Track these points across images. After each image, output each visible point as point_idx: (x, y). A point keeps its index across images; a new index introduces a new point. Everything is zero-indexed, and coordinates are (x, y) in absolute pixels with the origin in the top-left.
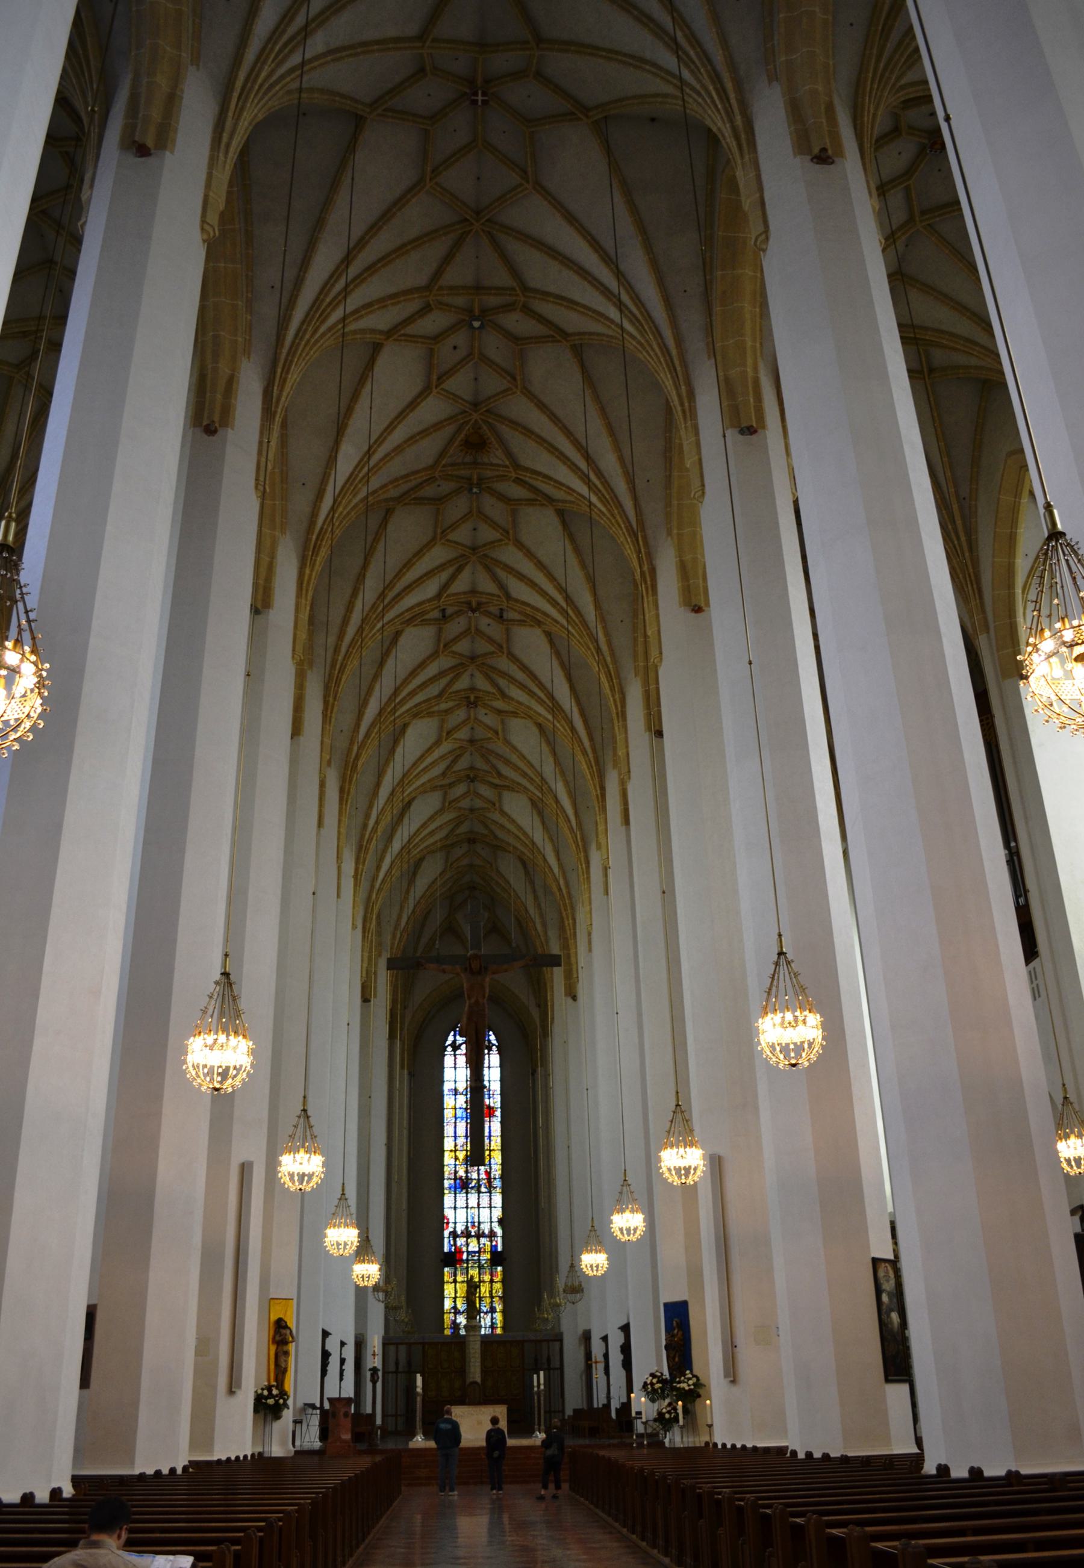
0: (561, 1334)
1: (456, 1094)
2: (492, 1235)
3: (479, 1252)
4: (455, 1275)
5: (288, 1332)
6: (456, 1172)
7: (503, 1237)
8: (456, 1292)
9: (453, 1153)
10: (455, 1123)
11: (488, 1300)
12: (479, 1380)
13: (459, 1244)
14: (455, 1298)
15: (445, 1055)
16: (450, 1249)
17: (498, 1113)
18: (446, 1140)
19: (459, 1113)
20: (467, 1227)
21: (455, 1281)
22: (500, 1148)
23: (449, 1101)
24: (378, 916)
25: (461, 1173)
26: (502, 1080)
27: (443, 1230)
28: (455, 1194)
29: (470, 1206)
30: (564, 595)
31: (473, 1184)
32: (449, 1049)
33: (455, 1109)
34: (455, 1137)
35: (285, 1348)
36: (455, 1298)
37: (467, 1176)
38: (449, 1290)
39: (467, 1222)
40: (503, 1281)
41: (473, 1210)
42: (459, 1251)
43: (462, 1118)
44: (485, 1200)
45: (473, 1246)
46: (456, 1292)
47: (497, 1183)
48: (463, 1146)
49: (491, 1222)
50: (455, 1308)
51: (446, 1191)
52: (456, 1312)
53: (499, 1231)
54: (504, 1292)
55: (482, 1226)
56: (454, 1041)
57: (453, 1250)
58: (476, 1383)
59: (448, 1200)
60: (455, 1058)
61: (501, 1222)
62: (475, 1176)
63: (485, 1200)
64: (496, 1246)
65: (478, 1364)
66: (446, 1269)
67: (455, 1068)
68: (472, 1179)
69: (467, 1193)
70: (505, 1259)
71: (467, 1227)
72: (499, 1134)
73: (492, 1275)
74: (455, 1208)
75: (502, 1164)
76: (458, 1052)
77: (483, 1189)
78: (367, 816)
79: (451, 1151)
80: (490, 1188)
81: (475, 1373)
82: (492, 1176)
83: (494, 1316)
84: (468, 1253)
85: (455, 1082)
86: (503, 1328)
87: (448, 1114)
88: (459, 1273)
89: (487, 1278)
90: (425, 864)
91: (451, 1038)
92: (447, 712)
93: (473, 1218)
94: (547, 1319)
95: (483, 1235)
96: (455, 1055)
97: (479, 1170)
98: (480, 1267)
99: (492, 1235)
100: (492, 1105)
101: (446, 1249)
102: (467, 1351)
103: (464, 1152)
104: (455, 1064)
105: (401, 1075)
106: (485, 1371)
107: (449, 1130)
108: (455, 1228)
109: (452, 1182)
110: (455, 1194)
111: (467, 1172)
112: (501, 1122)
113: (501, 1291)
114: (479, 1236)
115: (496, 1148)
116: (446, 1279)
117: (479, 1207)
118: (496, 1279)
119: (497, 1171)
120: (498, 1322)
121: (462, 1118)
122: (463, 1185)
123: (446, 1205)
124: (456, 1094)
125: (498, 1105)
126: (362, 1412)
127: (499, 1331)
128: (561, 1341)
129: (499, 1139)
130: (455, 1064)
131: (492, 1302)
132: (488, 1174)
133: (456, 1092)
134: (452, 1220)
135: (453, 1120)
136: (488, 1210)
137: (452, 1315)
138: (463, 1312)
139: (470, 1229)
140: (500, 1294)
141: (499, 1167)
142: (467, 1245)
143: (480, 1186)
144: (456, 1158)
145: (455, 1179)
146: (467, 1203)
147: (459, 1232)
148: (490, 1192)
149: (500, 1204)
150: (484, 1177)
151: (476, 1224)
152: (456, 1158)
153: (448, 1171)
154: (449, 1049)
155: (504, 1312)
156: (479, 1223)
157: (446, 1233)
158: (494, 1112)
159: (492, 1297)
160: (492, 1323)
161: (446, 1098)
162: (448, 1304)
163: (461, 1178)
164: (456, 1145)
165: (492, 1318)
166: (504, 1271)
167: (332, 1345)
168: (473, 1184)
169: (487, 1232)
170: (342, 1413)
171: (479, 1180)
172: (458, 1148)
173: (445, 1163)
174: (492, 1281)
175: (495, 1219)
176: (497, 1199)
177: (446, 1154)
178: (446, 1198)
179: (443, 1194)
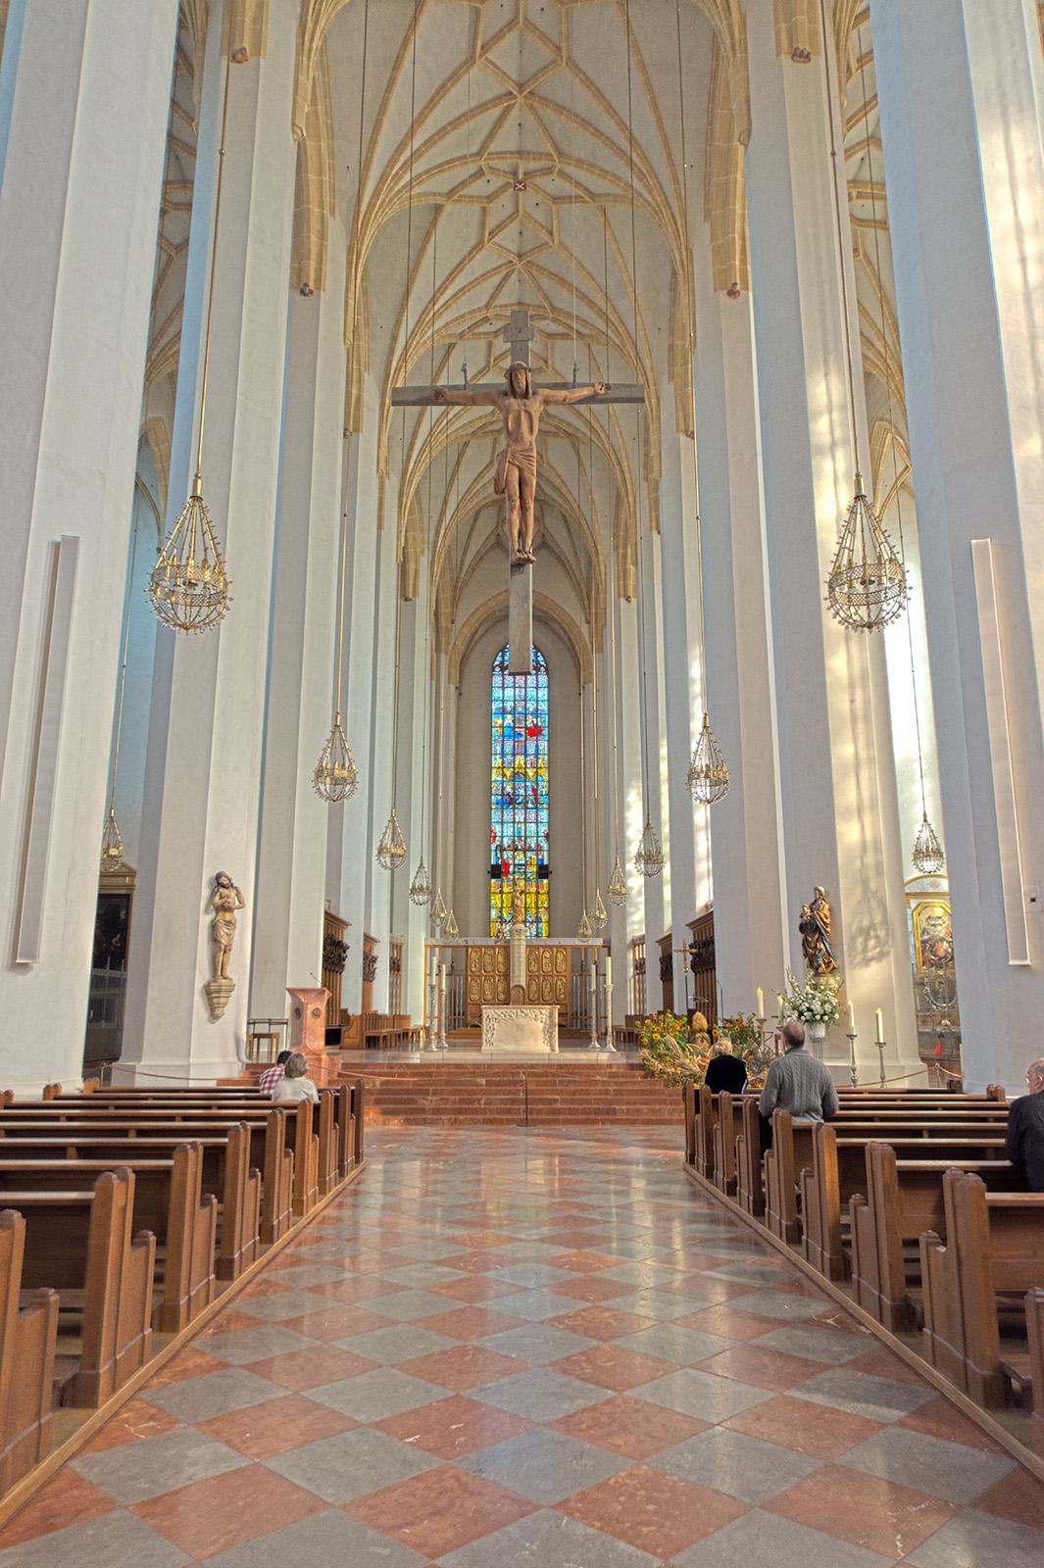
2: (538, 849)
3: (525, 865)
4: (501, 886)
5: (233, 893)
6: (503, 789)
7: (549, 851)
8: (502, 902)
9: (500, 771)
11: (534, 911)
12: (524, 984)
13: (505, 857)
14: (502, 908)
17: (545, 732)
20: (514, 841)
21: (501, 892)
24: (417, 492)
25: (509, 789)
30: (627, 133)
32: (497, 669)
35: (228, 917)
36: (502, 908)
37: (514, 793)
38: (496, 900)
42: (507, 866)
43: (509, 737)
44: (532, 815)
45: (520, 858)
46: (502, 902)
47: (543, 799)
49: (538, 837)
50: (501, 917)
52: (502, 921)
53: (545, 846)
56: (502, 662)
58: (520, 986)
59: (495, 816)
60: (504, 678)
61: (547, 837)
63: (532, 815)
64: (542, 860)
65: (523, 968)
66: (493, 881)
69: (514, 808)
71: (514, 841)
73: (537, 887)
74: (502, 823)
75: (549, 781)
78: (394, 338)
81: (520, 977)
84: (515, 865)
88: (505, 884)
89: (533, 889)
90: (469, 451)
91: (499, 659)
92: (491, 198)
95: (530, 849)
96: (503, 675)
98: (526, 879)
104: (503, 684)
105: (447, 689)
106: (530, 976)
111: (514, 788)
114: (525, 851)
116: (493, 889)
117: (525, 822)
118: (541, 891)
121: (509, 737)
122: (510, 801)
126: (374, 1008)
129: (546, 758)
130: (503, 684)
131: (537, 913)
132: (534, 790)
133: (503, 712)
134: (499, 834)
136: (533, 826)
141: (546, 784)
142: (514, 858)
144: (504, 775)
145: (502, 795)
148: (537, 808)
149: (545, 820)
154: (497, 669)
155: (549, 922)
156: (526, 837)
157: (493, 847)
158: (541, 731)
159: (537, 908)
160: (538, 932)
162: (494, 914)
163: (508, 794)
164: (503, 763)
165: (537, 928)
167: (352, 938)
169: (533, 846)
170: (309, 1012)
174: (537, 893)
175: (541, 834)
176: (544, 815)
177: (494, 771)
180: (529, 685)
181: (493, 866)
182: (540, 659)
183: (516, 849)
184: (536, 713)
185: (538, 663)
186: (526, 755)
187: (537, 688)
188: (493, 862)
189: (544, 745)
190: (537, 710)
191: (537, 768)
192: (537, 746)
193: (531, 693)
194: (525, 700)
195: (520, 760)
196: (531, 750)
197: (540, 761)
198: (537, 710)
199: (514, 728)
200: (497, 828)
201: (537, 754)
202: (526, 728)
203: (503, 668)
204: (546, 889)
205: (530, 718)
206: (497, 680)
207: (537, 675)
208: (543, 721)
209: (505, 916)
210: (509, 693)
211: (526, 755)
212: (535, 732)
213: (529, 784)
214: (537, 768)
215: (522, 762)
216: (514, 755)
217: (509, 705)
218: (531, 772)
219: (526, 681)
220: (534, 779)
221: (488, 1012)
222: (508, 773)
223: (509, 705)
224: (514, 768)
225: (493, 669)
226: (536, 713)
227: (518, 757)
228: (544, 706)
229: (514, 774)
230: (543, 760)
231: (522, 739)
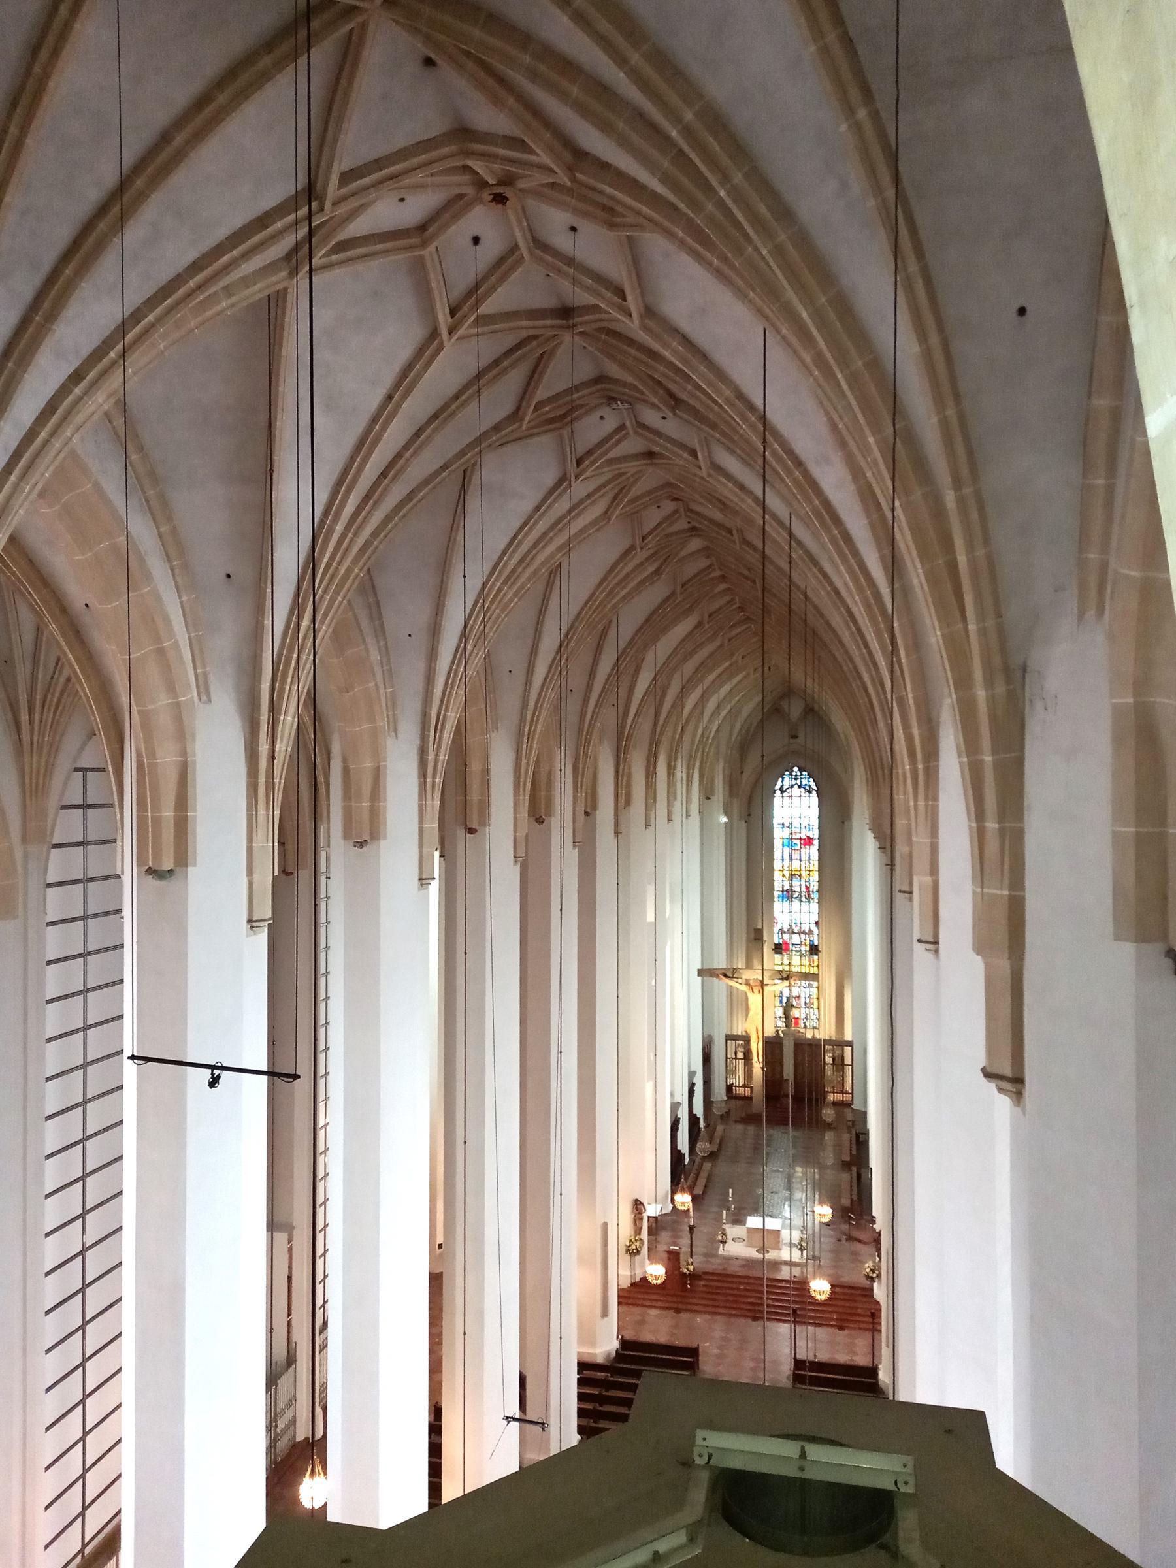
2: (811, 932)
3: (801, 944)
17: (816, 842)
18: (775, 862)
19: (786, 841)
20: (791, 926)
32: (778, 792)
34: (783, 860)
47: (816, 896)
55: (802, 926)
56: (782, 787)
61: (817, 923)
62: (797, 889)
71: (791, 926)
73: (810, 961)
76: (785, 794)
77: (803, 899)
80: (809, 899)
82: (811, 890)
95: (804, 933)
99: (811, 932)
109: (781, 893)
111: (791, 886)
119: (814, 886)
122: (789, 895)
125: (816, 836)
132: (807, 888)
139: (794, 928)
142: (791, 938)
143: (801, 896)
144: (784, 876)
145: (783, 891)
147: (786, 930)
148: (809, 902)
151: (799, 925)
152: (784, 876)
153: (777, 886)
157: (776, 930)
168: (796, 895)
176: (814, 906)
178: (775, 904)
181: (776, 945)
182: (812, 784)
183: (793, 933)
185: (810, 786)
197: (811, 865)
202: (801, 839)
203: (782, 791)
204: (816, 964)
205: (803, 831)
208: (815, 834)
212: (808, 841)
216: (791, 859)
218: (804, 874)
222: (787, 874)
225: (774, 792)
229: (792, 876)
230: (815, 865)
231: (798, 848)
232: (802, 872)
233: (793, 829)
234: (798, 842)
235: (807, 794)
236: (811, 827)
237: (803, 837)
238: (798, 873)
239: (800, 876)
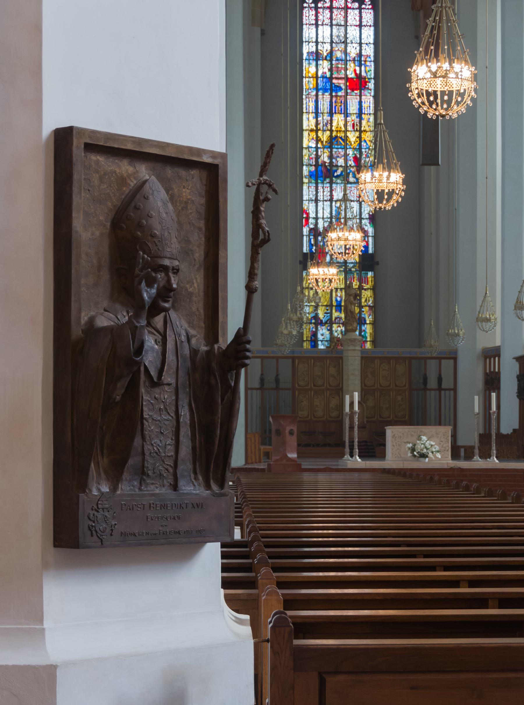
0: (456, 352)
1: (317, 60)
6: (317, 157)
7: (375, 237)
10: (317, 95)
15: (303, 8)
16: (311, 250)
17: (371, 85)
22: (372, 129)
23: (309, 69)
25: (325, 158)
26: (376, 43)
27: (302, 227)
28: (317, 184)
29: (335, 198)
31: (339, 172)
33: (317, 77)
37: (331, 163)
39: (331, 218)
40: (374, 289)
41: (338, 204)
48: (326, 124)
49: (361, 219)
50: (316, 317)
51: (305, 180)
54: (375, 301)
57: (313, 250)
59: (308, 192)
61: (372, 218)
62: (341, 162)
67: (317, 25)
68: (337, 166)
69: (331, 183)
70: (377, 263)
72: (372, 111)
73: (360, 280)
74: (316, 201)
76: (320, 5)
79: (312, 130)
83: (363, 328)
85: (317, 42)
86: (374, 342)
87: (308, 83)
93: (339, 213)
94: (458, 335)
96: (316, 8)
97: (346, 155)
100: (363, 74)
101: (305, 251)
102: (345, 367)
103: (328, 133)
104: (317, 20)
107: (309, 104)
108: (316, 224)
109: (313, 169)
110: (317, 184)
111: (331, 157)
112: (375, 97)
113: (371, 300)
115: (367, 129)
118: (366, 286)
120: (368, 335)
123: (305, 197)
124: (317, 60)
127: (368, 346)
128: (455, 359)
129: (372, 118)
130: (317, 20)
132: (357, 160)
133: (317, 56)
134: (312, 215)
135: (314, 93)
137: (312, 326)
138: (326, 323)
140: (370, 303)
143: (348, 174)
144: (318, 140)
145: (317, 165)
146: (331, 195)
150: (353, 164)
151: (342, 220)
152: (318, 140)
155: (374, 324)
157: (306, 230)
161: (305, 64)
164: (317, 124)
166: (375, 277)
168: (339, 172)
170: (287, 431)
171: (346, 167)
172: (320, 126)
173: (305, 145)
175: (365, 215)
177: (305, 134)
178: (305, 187)
179: (302, 183)
180: (350, 22)
184: (359, 59)
186: (346, 115)
187: (360, 26)
188: (305, 251)
189: (368, 100)
190: (360, 55)
191: (361, 132)
192: (360, 103)
193: (353, 33)
194: (345, 43)
195: (338, 120)
196: (353, 108)
197: (364, 123)
198: (360, 55)
199: (331, 78)
200: (310, 208)
201: (360, 114)
202: (347, 79)
206: (308, 15)
207: (360, 8)
209: (321, 316)
210: (325, 32)
211: (346, 115)
213: (350, 152)
214: (361, 132)
215: (342, 124)
217: (325, 49)
218: (352, 137)
219: (346, 17)
220: (356, 145)
221: (390, 431)
222: (325, 137)
223: (325, 49)
224: (331, 131)
226: (359, 59)
227: (336, 117)
228: (369, 51)
229: (332, 140)
232: (348, 134)
233: (334, 62)
234: (342, 83)
235: (356, 5)
236: (363, 59)
237: (351, 74)
238: (342, 135)
239: (346, 139)
